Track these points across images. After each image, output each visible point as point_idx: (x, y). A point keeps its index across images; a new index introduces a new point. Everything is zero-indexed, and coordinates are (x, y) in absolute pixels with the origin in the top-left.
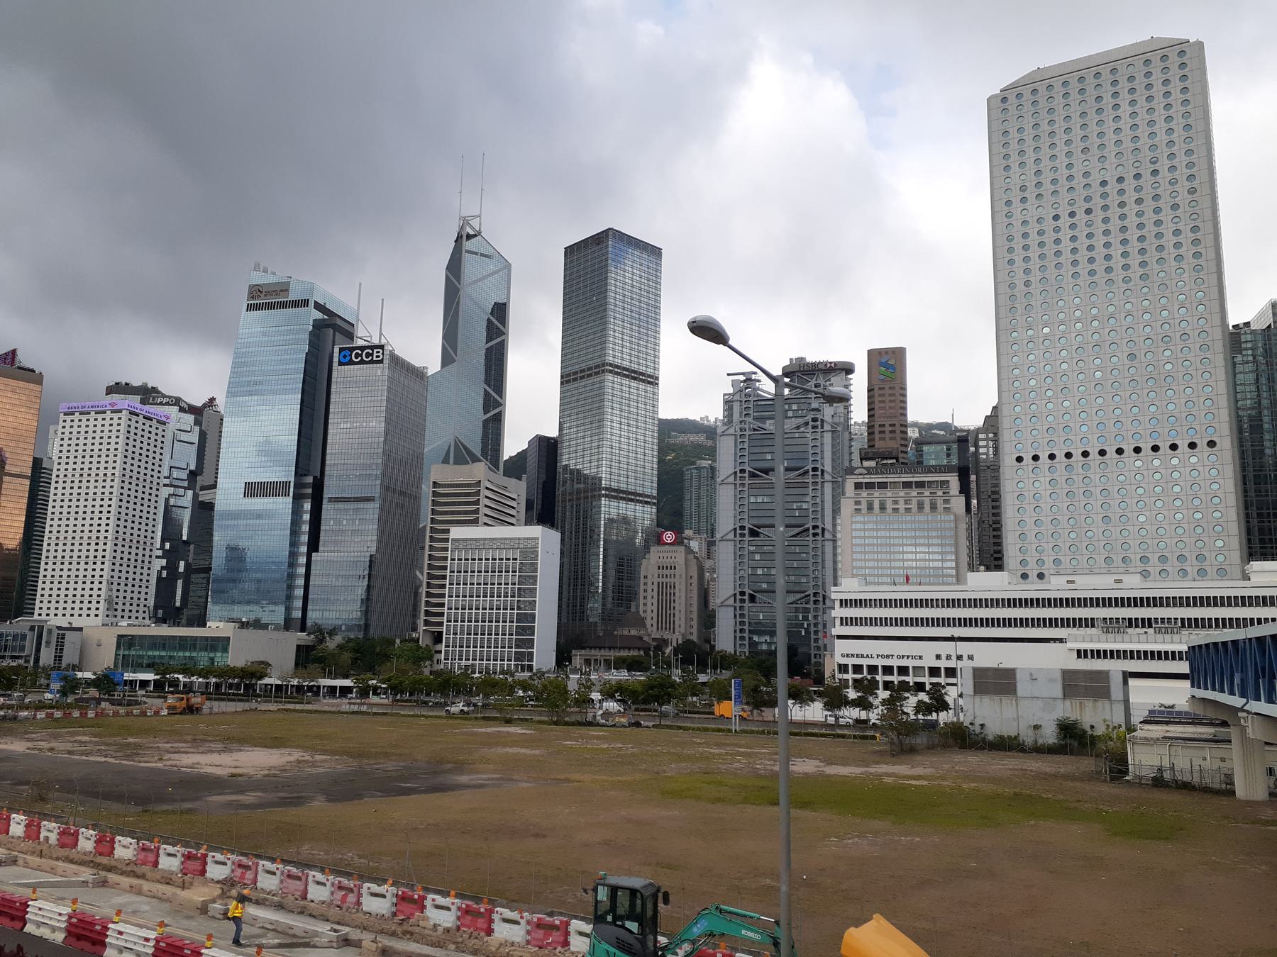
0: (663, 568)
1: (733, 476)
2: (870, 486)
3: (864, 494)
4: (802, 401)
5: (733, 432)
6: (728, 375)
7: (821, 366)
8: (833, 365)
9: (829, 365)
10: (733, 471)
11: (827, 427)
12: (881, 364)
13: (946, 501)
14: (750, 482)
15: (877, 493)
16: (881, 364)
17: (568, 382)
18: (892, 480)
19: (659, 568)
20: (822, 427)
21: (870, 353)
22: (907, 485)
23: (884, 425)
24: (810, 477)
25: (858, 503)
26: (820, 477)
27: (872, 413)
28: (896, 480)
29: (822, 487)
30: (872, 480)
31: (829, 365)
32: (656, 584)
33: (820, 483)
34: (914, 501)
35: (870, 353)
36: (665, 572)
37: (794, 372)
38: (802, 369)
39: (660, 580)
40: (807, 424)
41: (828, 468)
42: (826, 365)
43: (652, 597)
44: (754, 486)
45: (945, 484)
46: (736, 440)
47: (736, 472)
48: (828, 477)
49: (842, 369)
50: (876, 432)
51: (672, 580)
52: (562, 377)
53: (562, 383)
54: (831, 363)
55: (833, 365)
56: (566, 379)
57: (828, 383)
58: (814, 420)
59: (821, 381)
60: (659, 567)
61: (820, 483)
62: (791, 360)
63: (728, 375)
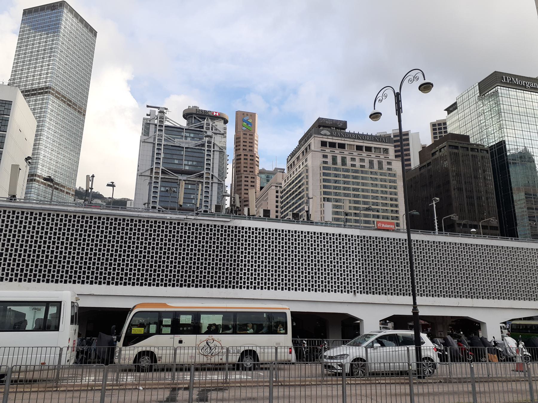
1: (150, 171)
2: (332, 145)
3: (328, 150)
4: (197, 132)
5: (152, 141)
6: (148, 106)
7: (209, 113)
8: (217, 114)
9: (215, 114)
10: (150, 167)
11: (216, 148)
12: (244, 121)
13: (389, 163)
14: (163, 177)
15: (337, 151)
16: (244, 121)
18: (348, 143)
20: (214, 148)
21: (237, 113)
22: (359, 148)
23: (247, 155)
24: (204, 178)
25: (325, 156)
26: (211, 179)
27: (238, 148)
28: (352, 143)
29: (212, 186)
30: (334, 141)
31: (215, 114)
33: (210, 184)
34: (367, 160)
35: (237, 113)
37: (192, 114)
38: (198, 113)
40: (203, 145)
41: (216, 174)
42: (213, 113)
45: (386, 151)
46: (154, 147)
47: (152, 169)
48: (215, 180)
49: (223, 119)
50: (242, 159)
54: (216, 113)
55: (217, 114)
57: (214, 124)
58: (209, 142)
59: (210, 121)
61: (210, 184)
62: (189, 107)
63: (148, 106)
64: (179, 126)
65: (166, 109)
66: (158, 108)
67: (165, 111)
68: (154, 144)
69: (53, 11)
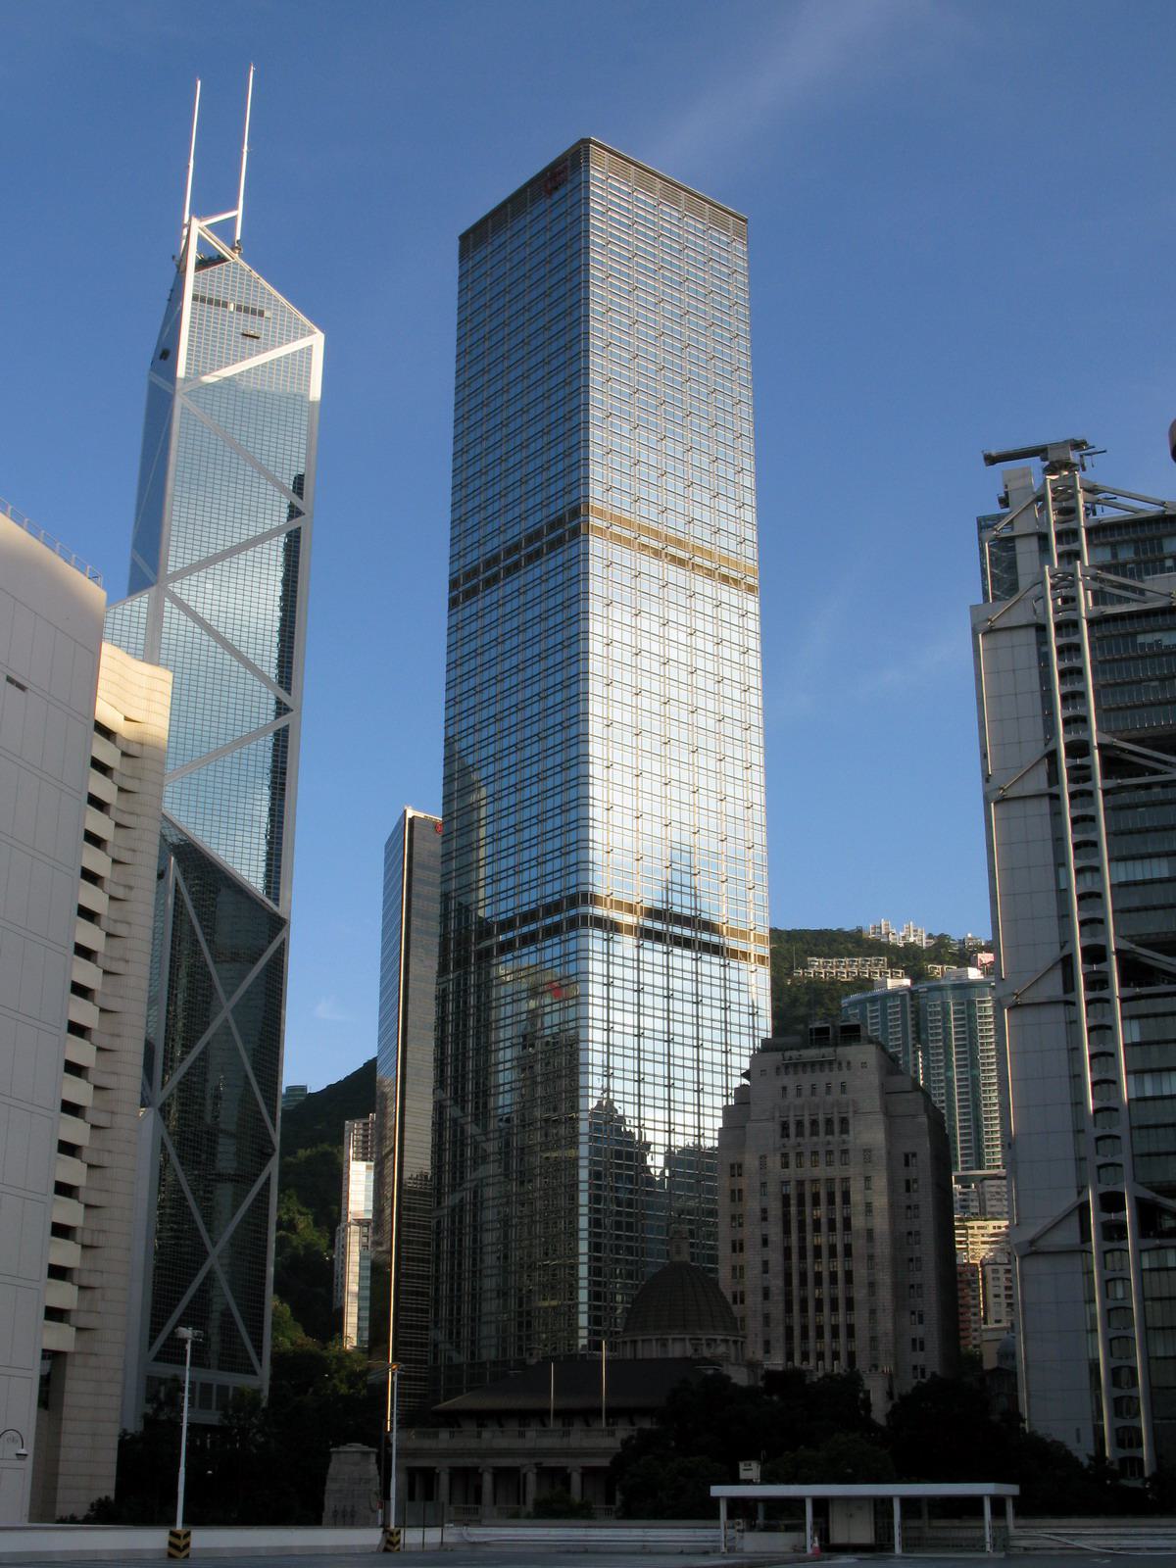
0: (800, 1133)
5: (1031, 618)
6: (991, 460)
17: (470, 594)
19: (785, 1133)
32: (773, 1188)
36: (807, 1141)
39: (792, 1173)
43: (765, 1242)
44: (1125, 798)
51: (836, 1172)
52: (454, 584)
53: (453, 603)
56: (464, 589)
60: (785, 1126)
63: (991, 460)
64: (1153, 510)
65: (1077, 445)
66: (1040, 452)
67: (1074, 457)
68: (1041, 629)
69: (556, 196)
